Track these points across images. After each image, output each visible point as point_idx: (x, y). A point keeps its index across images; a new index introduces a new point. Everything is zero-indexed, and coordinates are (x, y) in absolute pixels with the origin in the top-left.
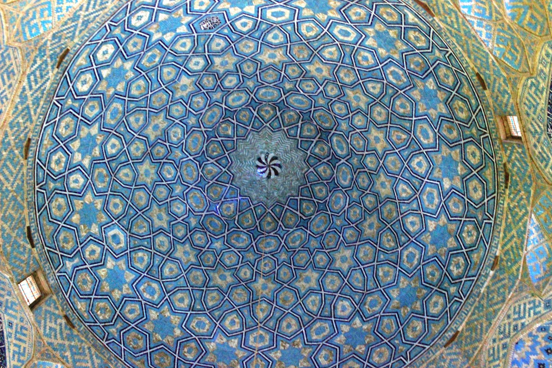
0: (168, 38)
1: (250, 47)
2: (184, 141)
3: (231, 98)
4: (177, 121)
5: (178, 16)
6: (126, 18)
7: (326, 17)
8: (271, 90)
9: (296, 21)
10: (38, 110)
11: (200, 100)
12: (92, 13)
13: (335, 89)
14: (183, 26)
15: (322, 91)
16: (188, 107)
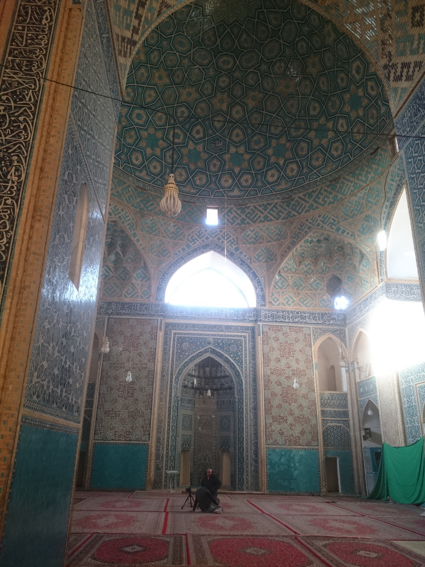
0: (242, 150)
1: (201, 109)
2: (277, 58)
3: (229, 67)
4: (273, 76)
5: (230, 163)
6: (251, 189)
7: (149, 132)
8: (199, 60)
9: (167, 127)
10: (315, 189)
11: (250, 80)
12: (260, 211)
13: (152, 59)
14: (231, 152)
15: (163, 54)
16: (260, 81)
